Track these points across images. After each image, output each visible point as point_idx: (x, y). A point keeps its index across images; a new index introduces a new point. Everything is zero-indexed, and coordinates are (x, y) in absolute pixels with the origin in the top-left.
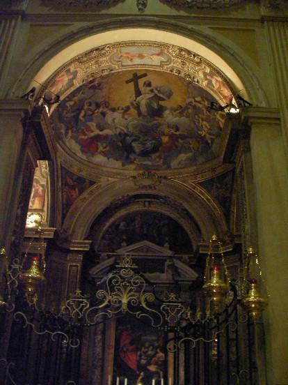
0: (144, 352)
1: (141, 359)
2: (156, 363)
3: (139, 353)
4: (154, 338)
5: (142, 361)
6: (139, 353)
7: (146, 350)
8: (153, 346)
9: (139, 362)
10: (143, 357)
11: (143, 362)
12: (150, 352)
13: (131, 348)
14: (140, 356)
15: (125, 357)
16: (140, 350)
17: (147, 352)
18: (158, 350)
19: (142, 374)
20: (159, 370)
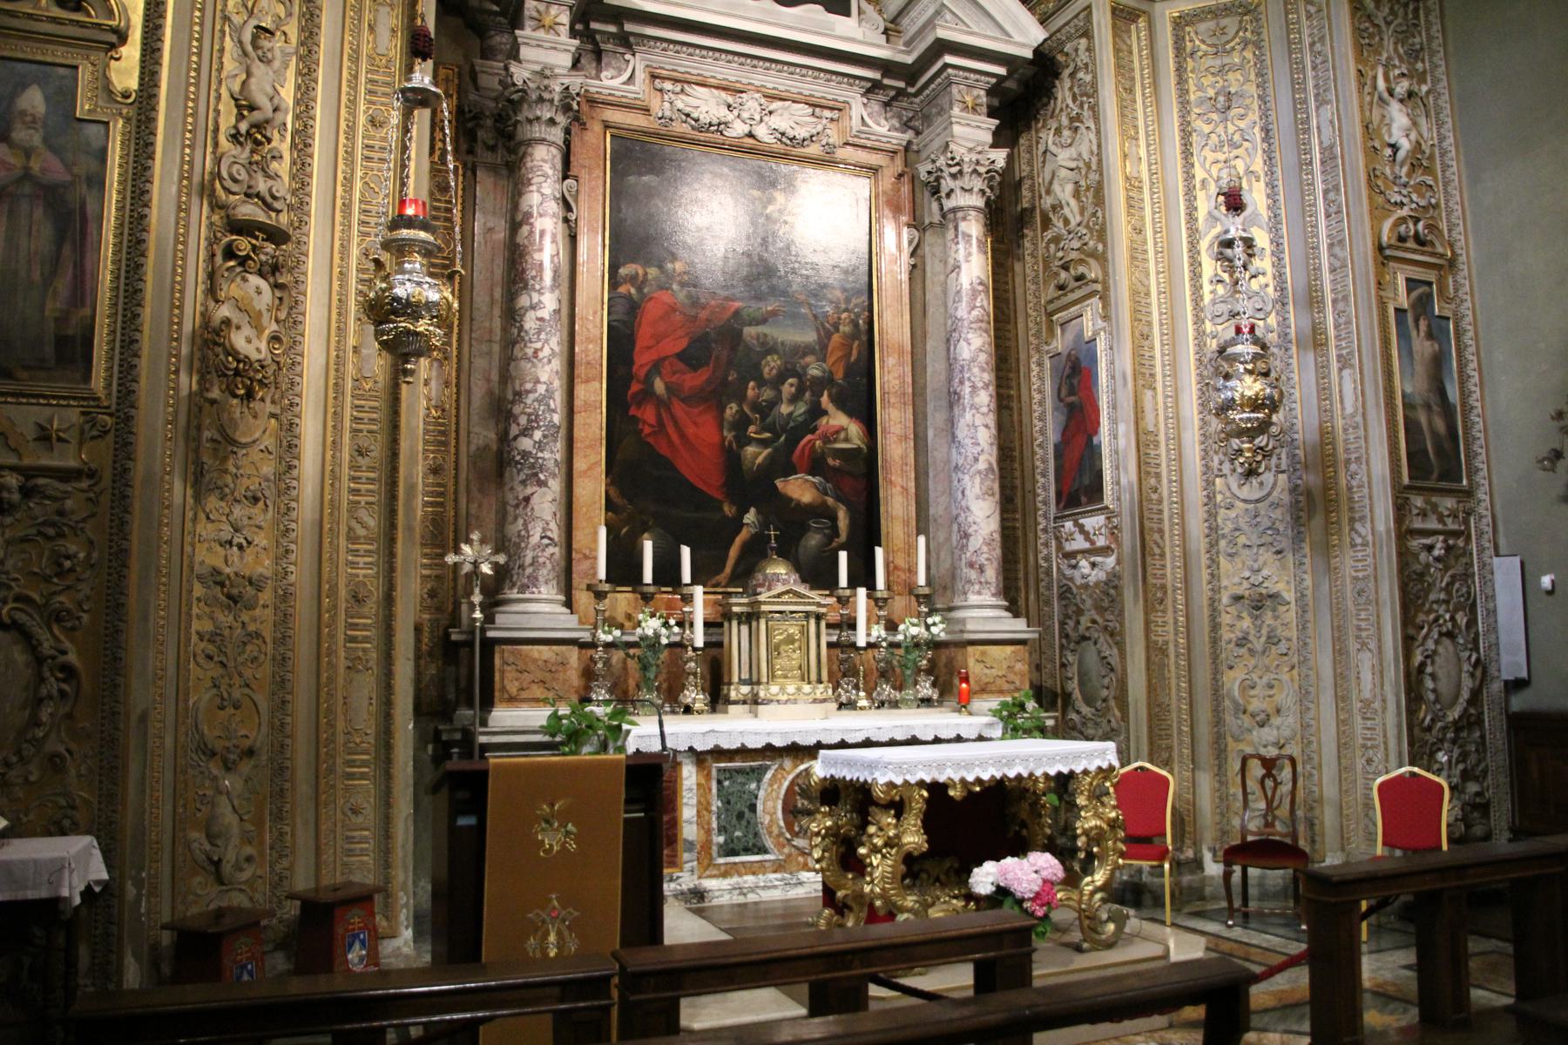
0: (756, 407)
1: (746, 441)
2: (816, 466)
3: (731, 410)
4: (809, 337)
5: (750, 450)
6: (731, 410)
7: (767, 394)
8: (800, 376)
9: (732, 458)
10: (752, 428)
11: (756, 455)
12: (785, 409)
13: (694, 380)
14: (741, 423)
15: (661, 424)
16: (741, 397)
17: (774, 403)
18: (825, 399)
19: (750, 517)
20: (830, 501)
